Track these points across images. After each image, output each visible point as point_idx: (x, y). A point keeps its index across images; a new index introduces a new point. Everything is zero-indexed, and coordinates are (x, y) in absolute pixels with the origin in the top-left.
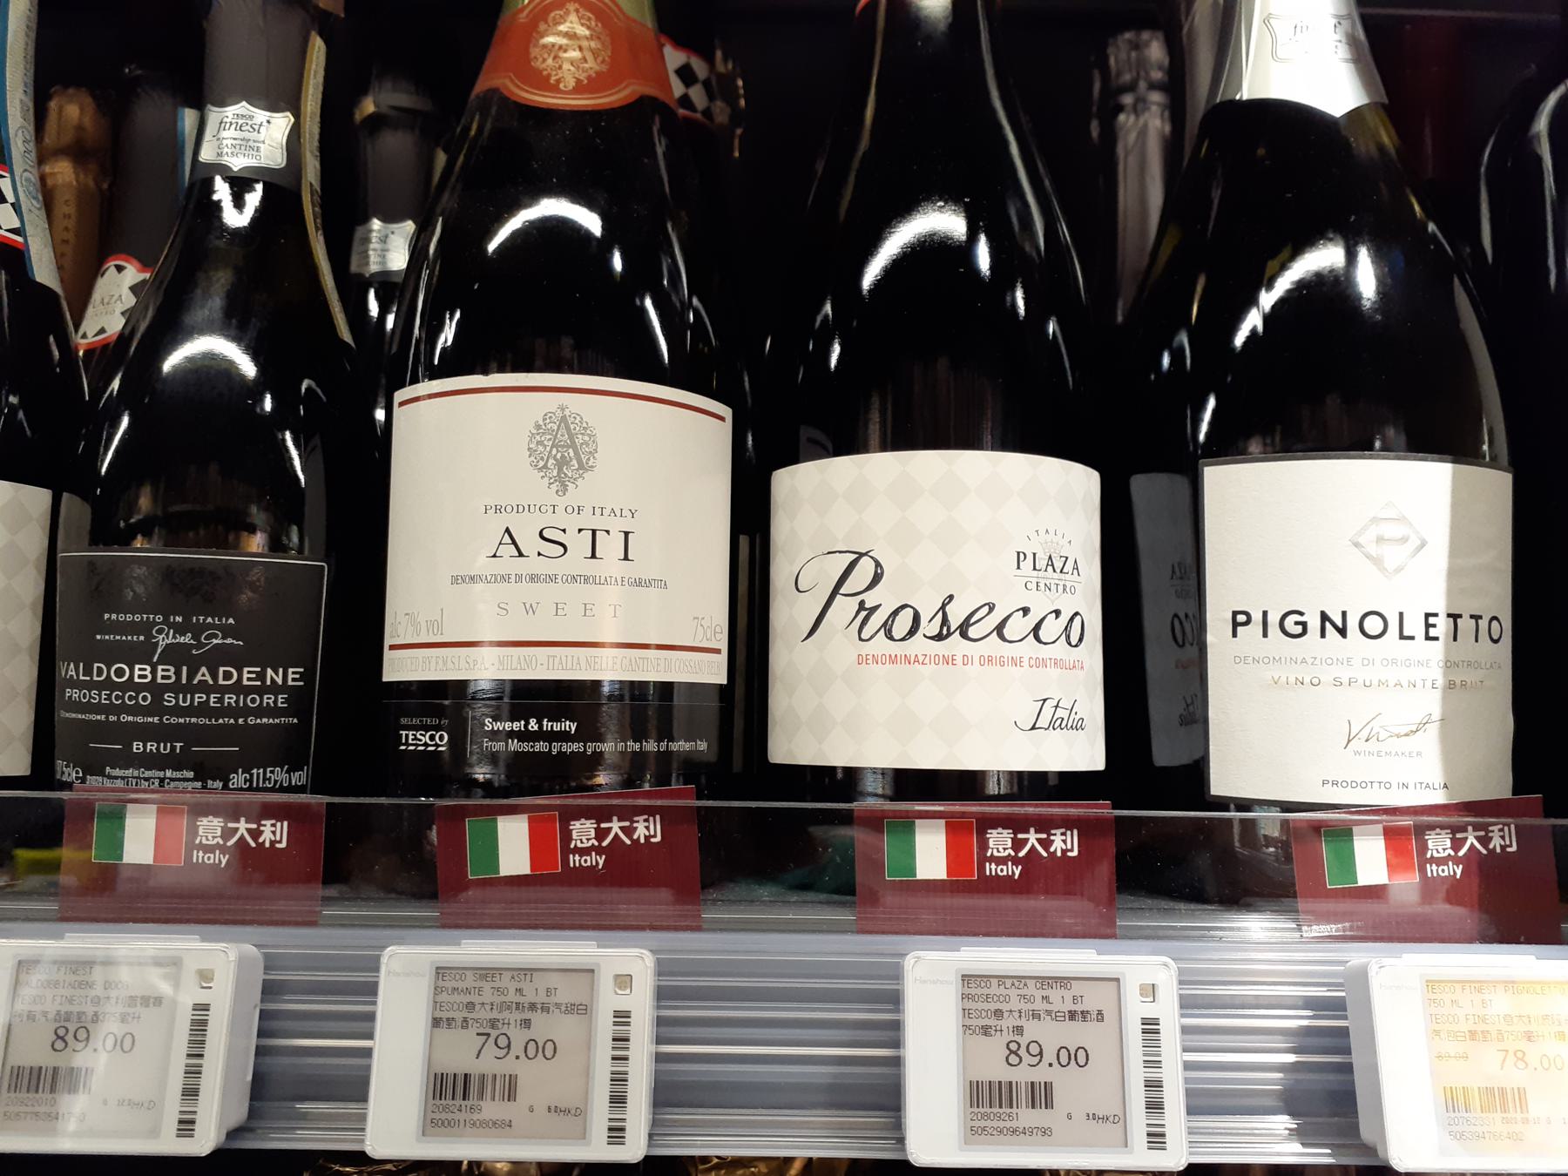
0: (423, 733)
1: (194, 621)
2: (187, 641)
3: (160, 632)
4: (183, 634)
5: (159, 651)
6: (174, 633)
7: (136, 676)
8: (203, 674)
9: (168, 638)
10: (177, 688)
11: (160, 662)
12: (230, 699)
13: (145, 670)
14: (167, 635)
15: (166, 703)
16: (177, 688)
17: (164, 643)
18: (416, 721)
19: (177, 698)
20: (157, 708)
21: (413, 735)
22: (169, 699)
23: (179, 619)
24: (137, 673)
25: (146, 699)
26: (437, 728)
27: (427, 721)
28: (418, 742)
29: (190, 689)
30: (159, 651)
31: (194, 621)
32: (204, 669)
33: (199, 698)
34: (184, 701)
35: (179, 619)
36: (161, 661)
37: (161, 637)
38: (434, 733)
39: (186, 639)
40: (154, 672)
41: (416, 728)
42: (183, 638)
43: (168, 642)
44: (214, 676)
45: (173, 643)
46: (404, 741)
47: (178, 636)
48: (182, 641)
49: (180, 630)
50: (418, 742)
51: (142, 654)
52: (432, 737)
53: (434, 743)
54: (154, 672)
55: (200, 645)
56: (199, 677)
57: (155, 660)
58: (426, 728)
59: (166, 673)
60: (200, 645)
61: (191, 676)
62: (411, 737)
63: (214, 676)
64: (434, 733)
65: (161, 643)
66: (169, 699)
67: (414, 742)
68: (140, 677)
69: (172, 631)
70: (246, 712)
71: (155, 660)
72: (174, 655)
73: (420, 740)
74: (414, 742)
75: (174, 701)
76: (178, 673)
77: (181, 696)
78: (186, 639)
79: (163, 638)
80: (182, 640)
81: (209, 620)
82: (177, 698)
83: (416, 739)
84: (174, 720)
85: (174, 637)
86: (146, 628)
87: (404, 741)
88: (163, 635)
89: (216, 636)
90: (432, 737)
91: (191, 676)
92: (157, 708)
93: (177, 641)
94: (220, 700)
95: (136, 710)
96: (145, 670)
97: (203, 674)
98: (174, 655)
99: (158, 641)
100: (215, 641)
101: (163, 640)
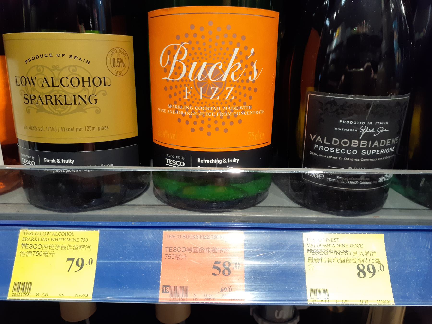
0: (175, 161)
1: (376, 124)
2: (372, 131)
4: (371, 129)
5: (362, 135)
6: (368, 129)
7: (361, 145)
8: (376, 144)
9: (366, 131)
10: (367, 149)
11: (362, 139)
13: (365, 142)
14: (366, 129)
15: (362, 154)
17: (364, 132)
18: (172, 156)
19: (366, 152)
20: (359, 155)
21: (171, 161)
22: (364, 152)
23: (371, 123)
26: (181, 160)
27: (176, 157)
28: (173, 164)
30: (362, 135)
31: (376, 124)
34: (369, 153)
35: (371, 123)
37: (363, 130)
38: (179, 162)
39: (373, 131)
41: (172, 159)
42: (371, 130)
43: (366, 132)
45: (367, 132)
46: (167, 162)
47: (369, 129)
48: (371, 131)
49: (370, 127)
50: (173, 164)
52: (178, 163)
53: (179, 165)
56: (375, 145)
57: (360, 138)
58: (176, 160)
59: (364, 143)
61: (372, 144)
62: (170, 162)
63: (379, 144)
64: (179, 162)
65: (363, 132)
67: (172, 164)
68: (354, 145)
69: (368, 128)
71: (360, 138)
73: (174, 164)
74: (172, 164)
75: (365, 153)
77: (368, 151)
78: (373, 131)
79: (364, 130)
80: (371, 131)
81: (381, 123)
82: (366, 152)
83: (172, 162)
85: (368, 130)
87: (167, 162)
88: (364, 129)
90: (178, 163)
91: (372, 144)
92: (359, 155)
93: (369, 131)
95: (351, 156)
96: (365, 142)
98: (368, 137)
99: (362, 131)
100: (381, 131)
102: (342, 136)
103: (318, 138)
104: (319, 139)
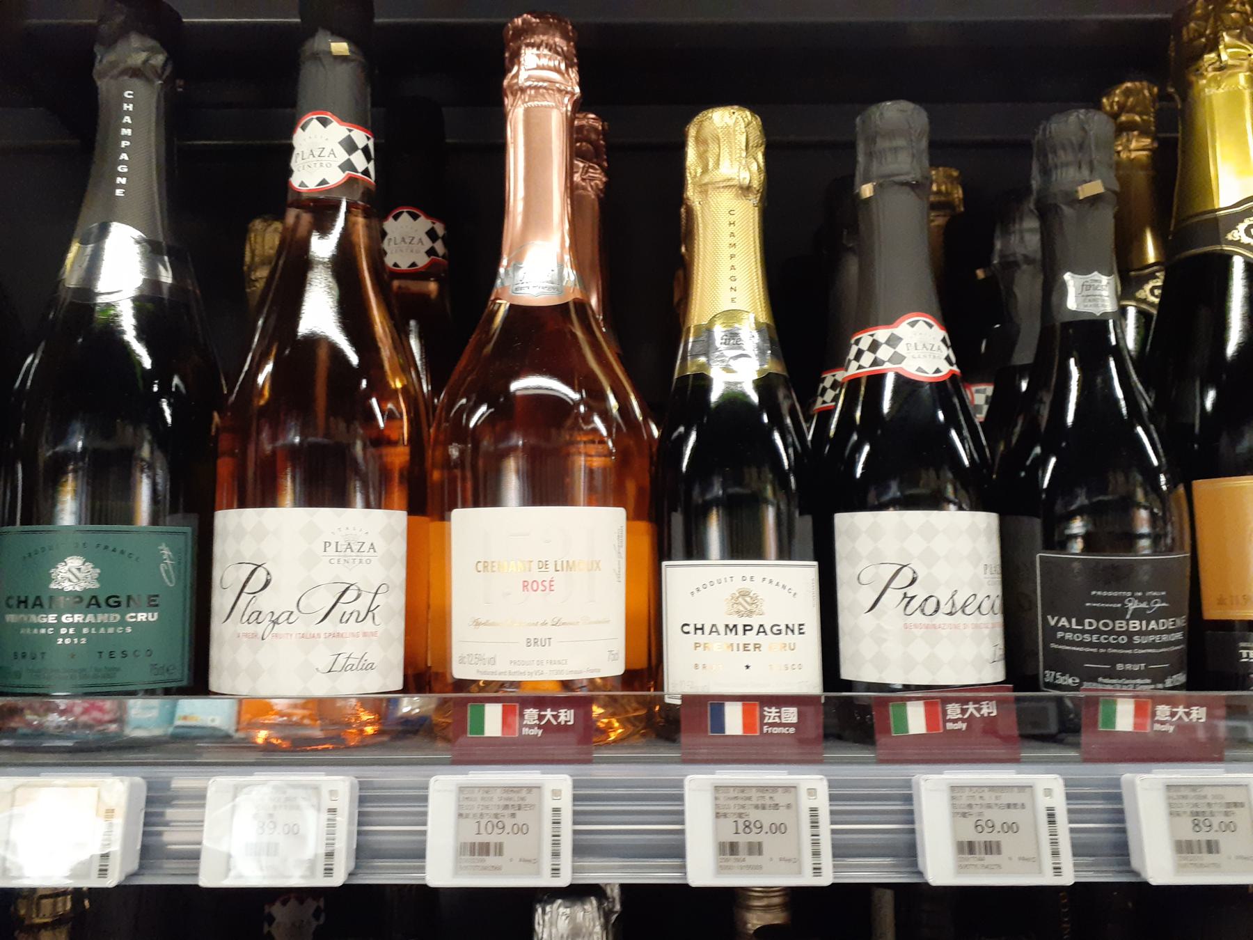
3: (1130, 601)
8: (1153, 625)
23: (1140, 594)
24: (1117, 625)
25: (1123, 640)
35: (1140, 594)
36: (1131, 618)
39: (1144, 605)
49: (1141, 600)
51: (1119, 614)
54: (1128, 624)
59: (1135, 625)
66: (1137, 639)
70: (1109, 645)
72: (1138, 615)
76: (1141, 625)
78: (1144, 605)
86: (1121, 600)
89: (1156, 603)
92: (1130, 645)
95: (1118, 646)
101: (1132, 606)
102: (1098, 614)
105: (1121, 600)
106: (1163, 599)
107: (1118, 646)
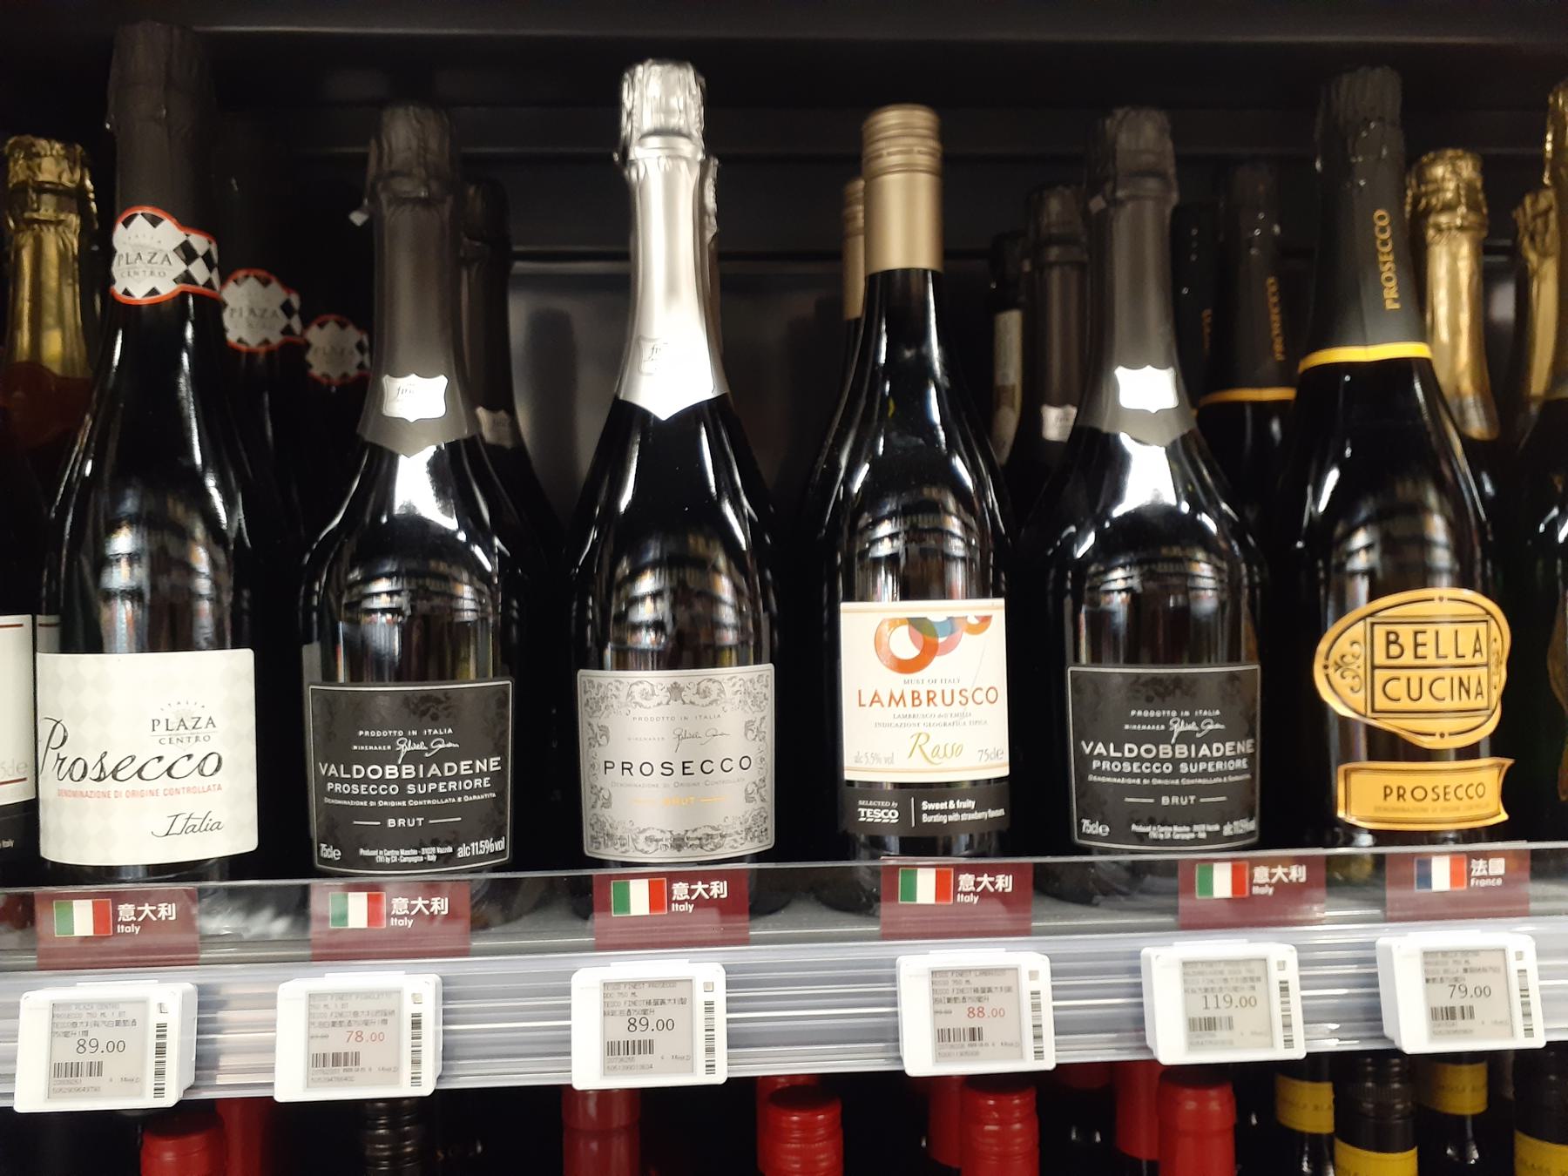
3: (401, 742)
12: (452, 785)
14: (407, 744)
16: (416, 781)
23: (415, 733)
24: (387, 772)
25: (394, 790)
29: (426, 780)
30: (402, 756)
32: (434, 766)
33: (432, 786)
35: (415, 733)
36: (405, 762)
37: (403, 746)
39: (421, 746)
40: (400, 771)
44: (442, 772)
49: (415, 740)
54: (400, 771)
55: (430, 750)
59: (408, 771)
60: (430, 750)
61: (426, 771)
69: (410, 741)
70: (378, 797)
76: (417, 770)
78: (421, 746)
81: (436, 732)
84: (416, 803)
86: (391, 740)
92: (403, 795)
94: (446, 787)
95: (388, 797)
97: (434, 770)
101: (404, 748)
102: (365, 759)
103: (432, 769)
104: (434, 770)
105: (391, 740)
106: (447, 738)
107: (388, 797)
